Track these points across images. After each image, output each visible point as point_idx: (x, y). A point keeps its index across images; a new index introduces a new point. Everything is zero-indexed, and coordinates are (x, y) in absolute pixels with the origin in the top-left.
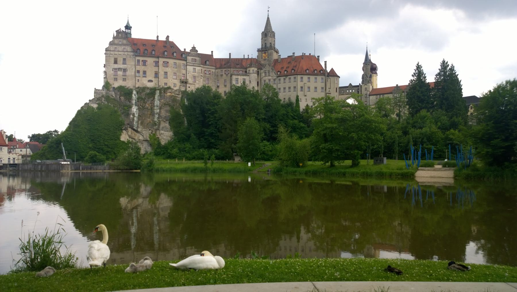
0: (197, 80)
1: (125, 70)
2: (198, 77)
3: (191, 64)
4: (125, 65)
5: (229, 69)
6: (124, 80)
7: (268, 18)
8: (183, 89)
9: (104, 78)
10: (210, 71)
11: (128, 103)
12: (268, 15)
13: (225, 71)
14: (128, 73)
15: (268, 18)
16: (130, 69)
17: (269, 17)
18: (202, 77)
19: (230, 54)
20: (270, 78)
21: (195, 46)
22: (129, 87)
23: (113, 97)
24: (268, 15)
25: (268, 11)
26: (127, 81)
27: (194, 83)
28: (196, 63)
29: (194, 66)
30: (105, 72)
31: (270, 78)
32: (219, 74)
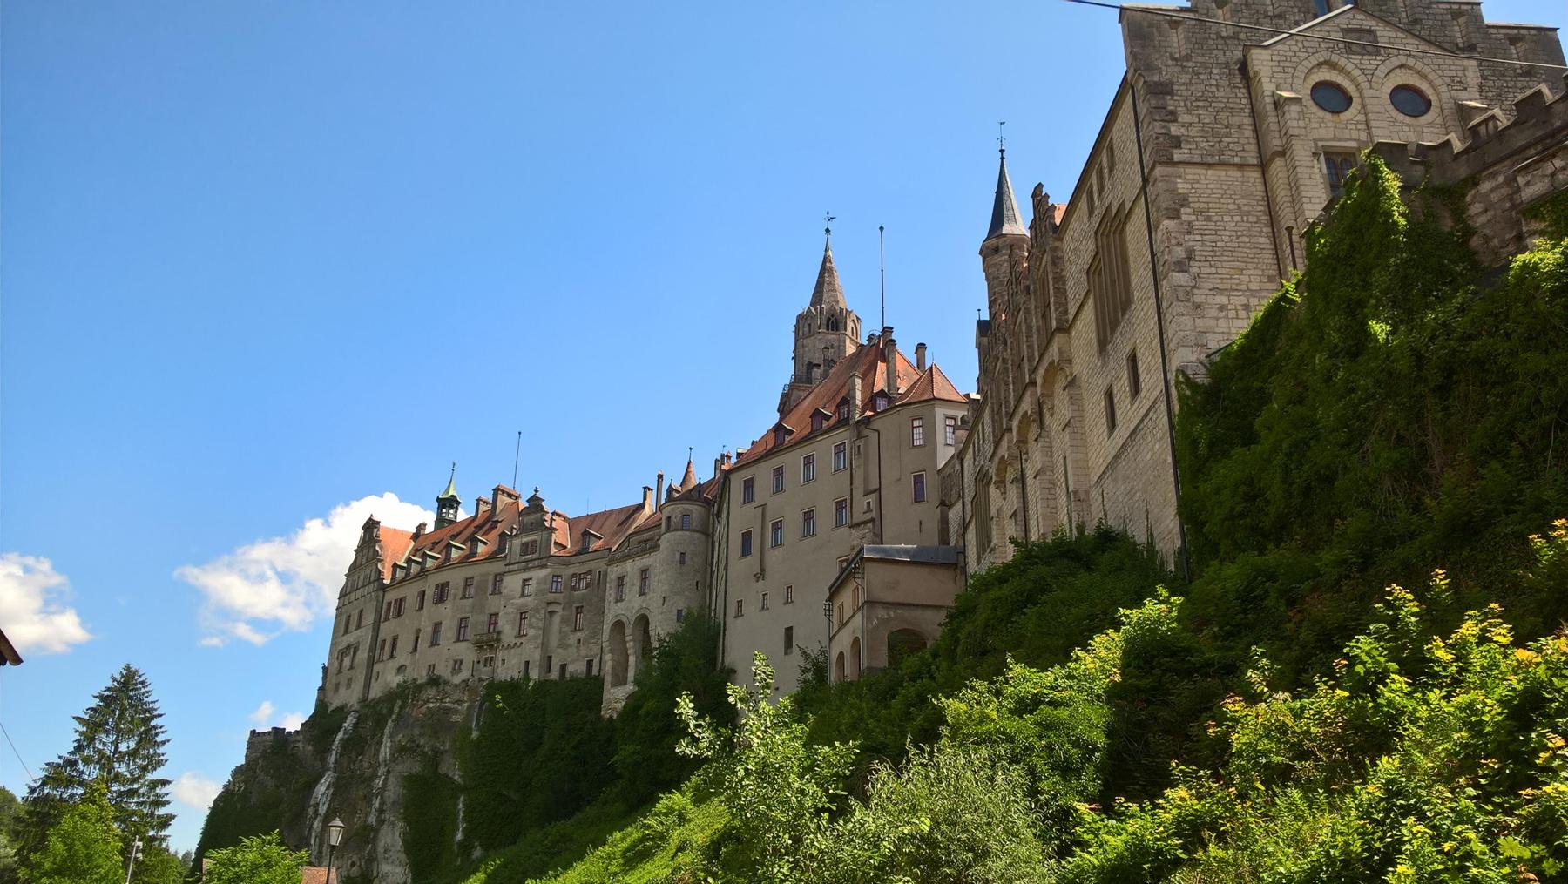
0: (531, 626)
2: (537, 610)
3: (516, 567)
7: (826, 259)
8: (485, 672)
9: (320, 689)
10: (589, 572)
11: (318, 764)
15: (826, 259)
17: (830, 253)
18: (551, 608)
21: (538, 495)
24: (826, 251)
27: (518, 641)
28: (535, 556)
29: (524, 570)
30: (325, 669)
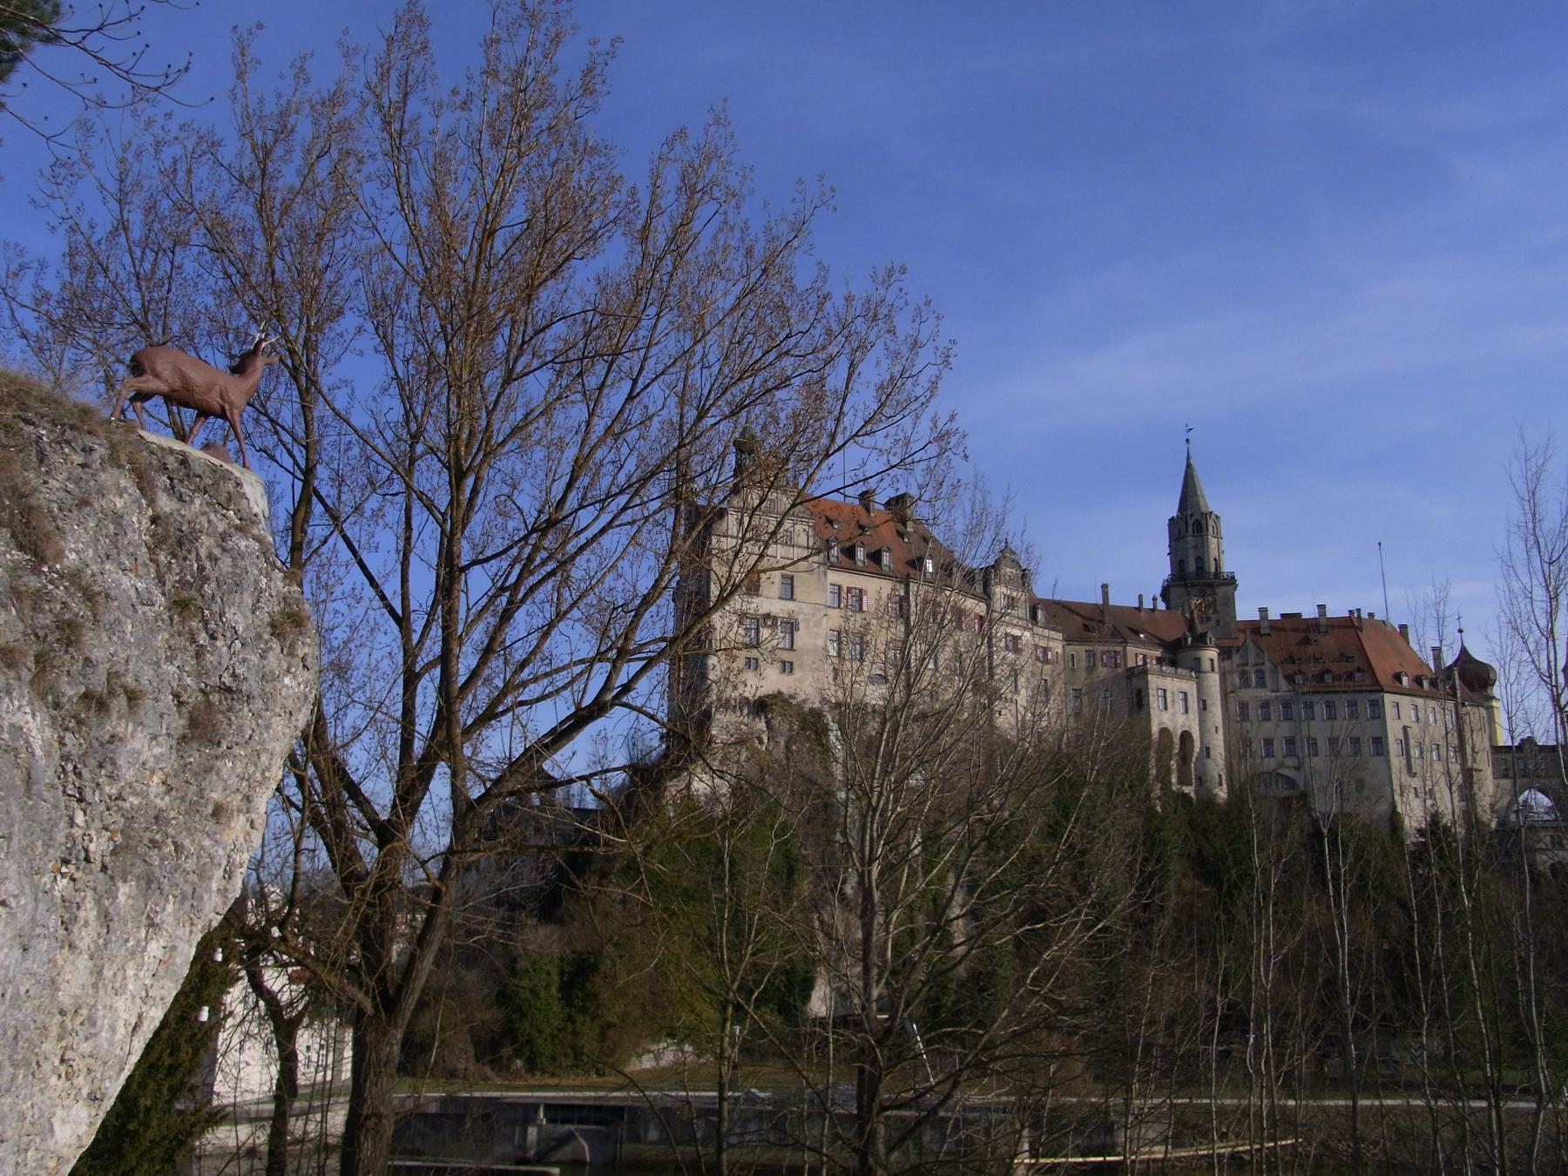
1: (792, 626)
4: (790, 605)
5: (1119, 649)
6: (787, 667)
7: (1189, 466)
12: (1188, 458)
13: (1103, 653)
14: (801, 638)
15: (1189, 466)
16: (807, 620)
19: (1105, 587)
20: (1264, 694)
22: (804, 701)
23: (761, 742)
24: (1188, 458)
25: (1187, 441)
26: (798, 673)
31: (1264, 694)
32: (1079, 660)
